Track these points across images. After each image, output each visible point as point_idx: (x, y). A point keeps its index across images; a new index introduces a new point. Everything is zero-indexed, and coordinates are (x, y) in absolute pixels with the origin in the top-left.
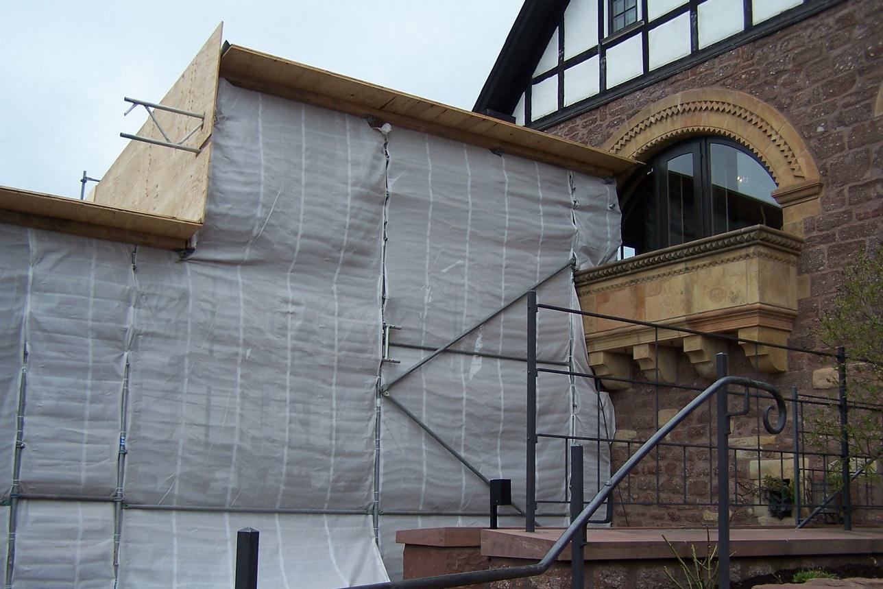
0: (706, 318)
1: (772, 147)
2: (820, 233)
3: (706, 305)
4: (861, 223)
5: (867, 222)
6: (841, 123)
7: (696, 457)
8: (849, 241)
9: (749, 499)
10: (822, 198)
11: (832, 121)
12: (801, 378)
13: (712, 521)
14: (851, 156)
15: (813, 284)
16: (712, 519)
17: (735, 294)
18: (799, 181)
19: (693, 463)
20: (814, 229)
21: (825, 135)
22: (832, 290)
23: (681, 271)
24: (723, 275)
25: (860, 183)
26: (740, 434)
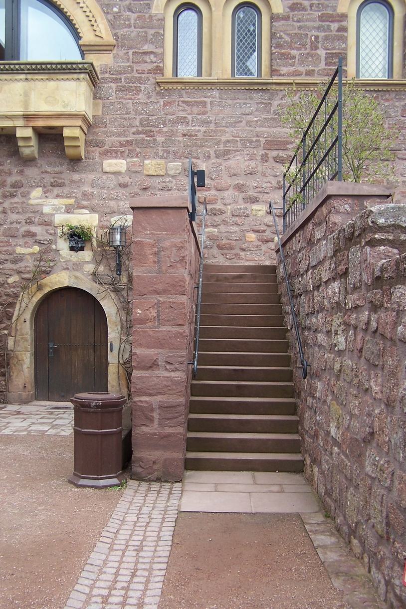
0: (40, 115)
1: (80, 11)
2: (111, 76)
3: (40, 106)
4: (139, 75)
5: (143, 76)
6: (130, 10)
7: (9, 211)
8: (131, 85)
9: (53, 239)
10: (113, 54)
11: (124, 7)
12: (94, 165)
13: (23, 254)
14: (135, 33)
15: (104, 107)
16: (23, 253)
17: (66, 102)
18: (98, 39)
19: (7, 215)
20: (106, 72)
21: (118, 14)
22: (117, 113)
23: (21, 79)
24: (57, 88)
25: (140, 51)
26: (47, 197)
